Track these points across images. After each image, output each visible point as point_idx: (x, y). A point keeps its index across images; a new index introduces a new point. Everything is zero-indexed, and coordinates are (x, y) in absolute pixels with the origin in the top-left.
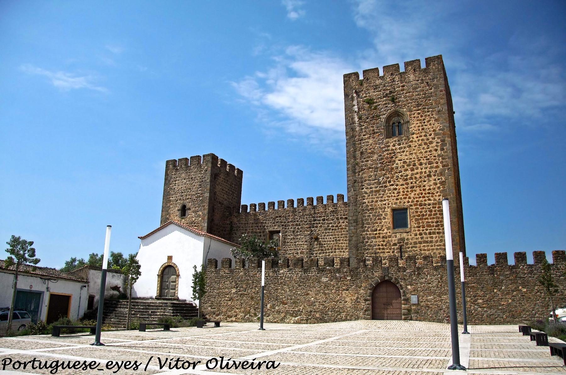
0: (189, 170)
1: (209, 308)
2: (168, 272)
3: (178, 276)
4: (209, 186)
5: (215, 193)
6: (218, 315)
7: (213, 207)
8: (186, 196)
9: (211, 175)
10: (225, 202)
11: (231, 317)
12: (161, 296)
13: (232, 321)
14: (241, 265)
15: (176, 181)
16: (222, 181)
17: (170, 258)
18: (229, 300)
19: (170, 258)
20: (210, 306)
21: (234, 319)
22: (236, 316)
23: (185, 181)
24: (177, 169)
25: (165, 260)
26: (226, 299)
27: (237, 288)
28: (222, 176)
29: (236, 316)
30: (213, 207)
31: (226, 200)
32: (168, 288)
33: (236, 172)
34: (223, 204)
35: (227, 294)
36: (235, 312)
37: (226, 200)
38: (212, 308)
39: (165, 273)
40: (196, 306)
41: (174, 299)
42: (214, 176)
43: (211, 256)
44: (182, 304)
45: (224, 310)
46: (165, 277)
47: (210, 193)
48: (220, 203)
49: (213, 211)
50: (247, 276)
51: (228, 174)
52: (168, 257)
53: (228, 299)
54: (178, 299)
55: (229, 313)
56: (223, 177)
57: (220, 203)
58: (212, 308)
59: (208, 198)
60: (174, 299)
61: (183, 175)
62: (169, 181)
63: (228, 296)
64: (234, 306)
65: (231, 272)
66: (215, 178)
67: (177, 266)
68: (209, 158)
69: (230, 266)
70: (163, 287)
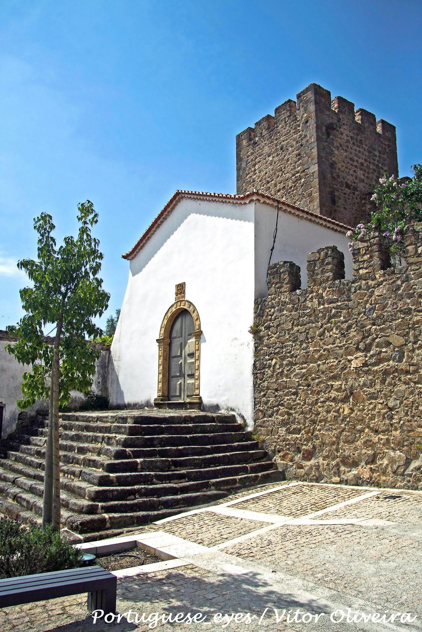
0: (276, 134)
1: (282, 431)
2: (180, 326)
3: (199, 335)
4: (315, 151)
5: (332, 165)
6: (308, 456)
7: (332, 193)
8: (275, 185)
9: (318, 128)
10: (361, 186)
11: (355, 464)
12: (165, 399)
13: (358, 481)
14: (376, 261)
15: (254, 165)
16: (348, 141)
17: (181, 289)
18: (345, 400)
19: (181, 289)
20: (284, 423)
21: (364, 470)
22: (372, 460)
23: (271, 158)
24: (255, 143)
25: (172, 299)
26: (333, 394)
27: (367, 349)
28: (345, 133)
29: (372, 460)
30: (332, 193)
31: (363, 181)
32: (182, 375)
33: (379, 129)
34: (355, 189)
35: (334, 378)
36: (368, 444)
37: (363, 181)
38: (289, 432)
39: (174, 334)
40: (246, 425)
41: (192, 405)
42: (327, 131)
43: (277, 259)
44: (205, 419)
45: (330, 436)
46: (176, 343)
47: (320, 163)
48: (348, 186)
49: (334, 202)
50: (401, 297)
51: (359, 128)
52: (178, 286)
53: (341, 395)
54: (200, 405)
55: (347, 450)
56: (346, 132)
57: (348, 186)
58: (289, 432)
59: (316, 174)
60: (192, 405)
61: (266, 149)
62: (244, 169)
63: (337, 383)
64: (362, 421)
65: (341, 292)
66: (328, 134)
67: (195, 309)
68: (310, 95)
69: (339, 274)
70: (175, 371)
